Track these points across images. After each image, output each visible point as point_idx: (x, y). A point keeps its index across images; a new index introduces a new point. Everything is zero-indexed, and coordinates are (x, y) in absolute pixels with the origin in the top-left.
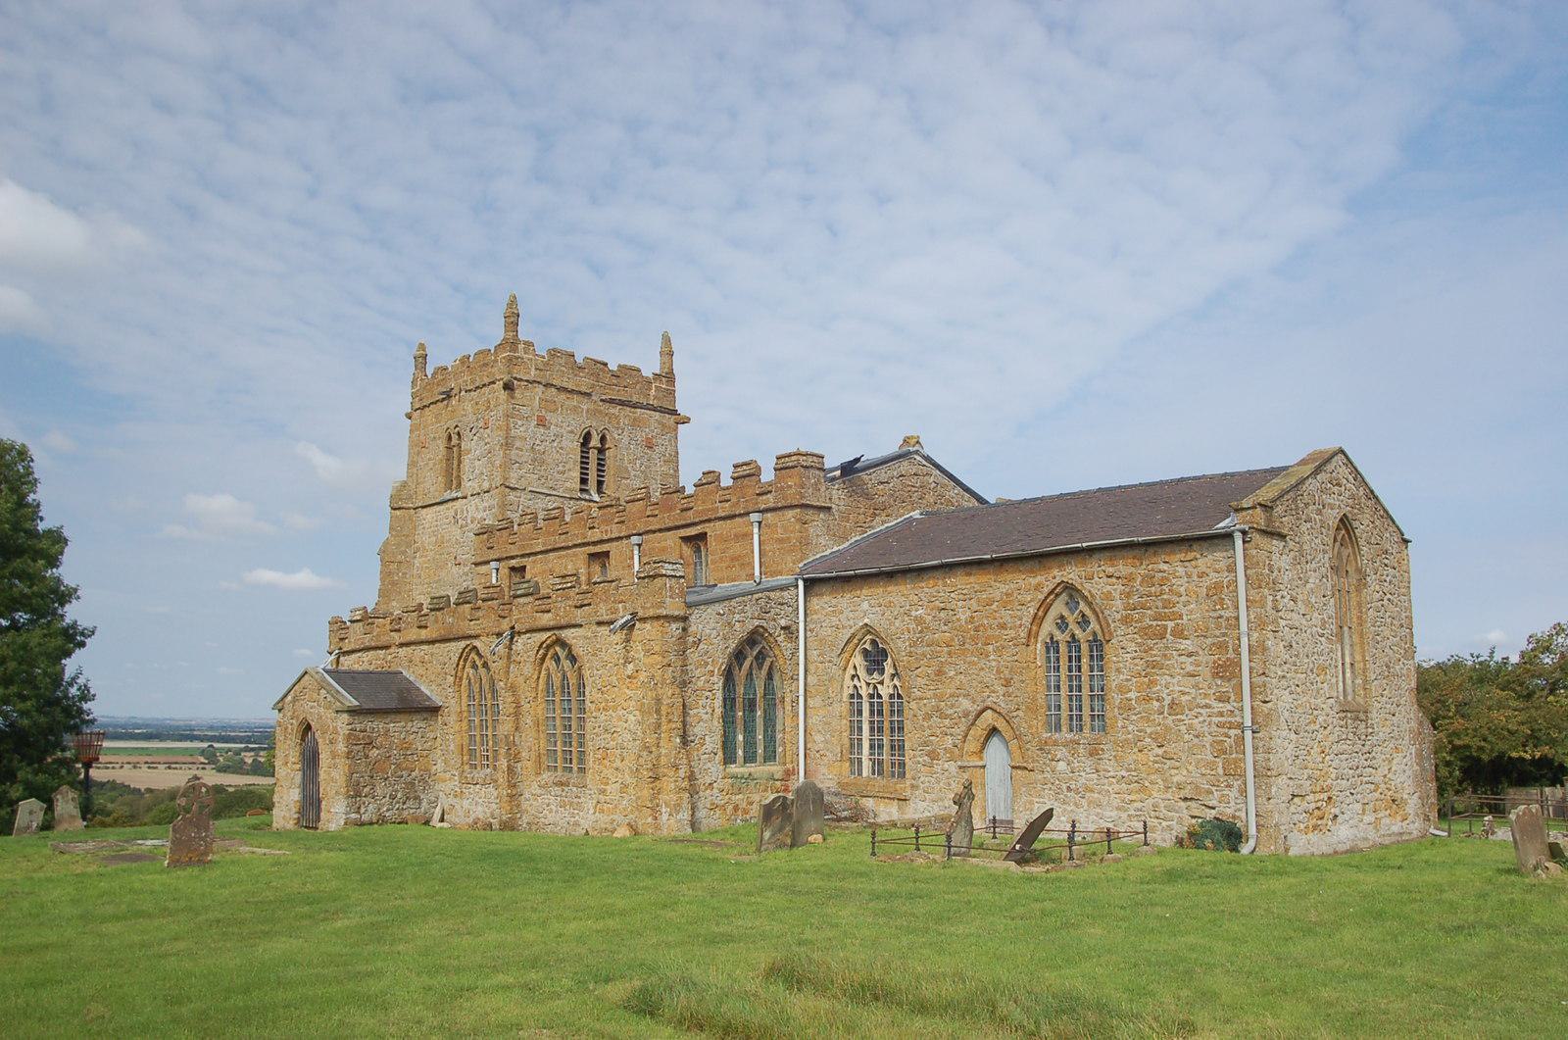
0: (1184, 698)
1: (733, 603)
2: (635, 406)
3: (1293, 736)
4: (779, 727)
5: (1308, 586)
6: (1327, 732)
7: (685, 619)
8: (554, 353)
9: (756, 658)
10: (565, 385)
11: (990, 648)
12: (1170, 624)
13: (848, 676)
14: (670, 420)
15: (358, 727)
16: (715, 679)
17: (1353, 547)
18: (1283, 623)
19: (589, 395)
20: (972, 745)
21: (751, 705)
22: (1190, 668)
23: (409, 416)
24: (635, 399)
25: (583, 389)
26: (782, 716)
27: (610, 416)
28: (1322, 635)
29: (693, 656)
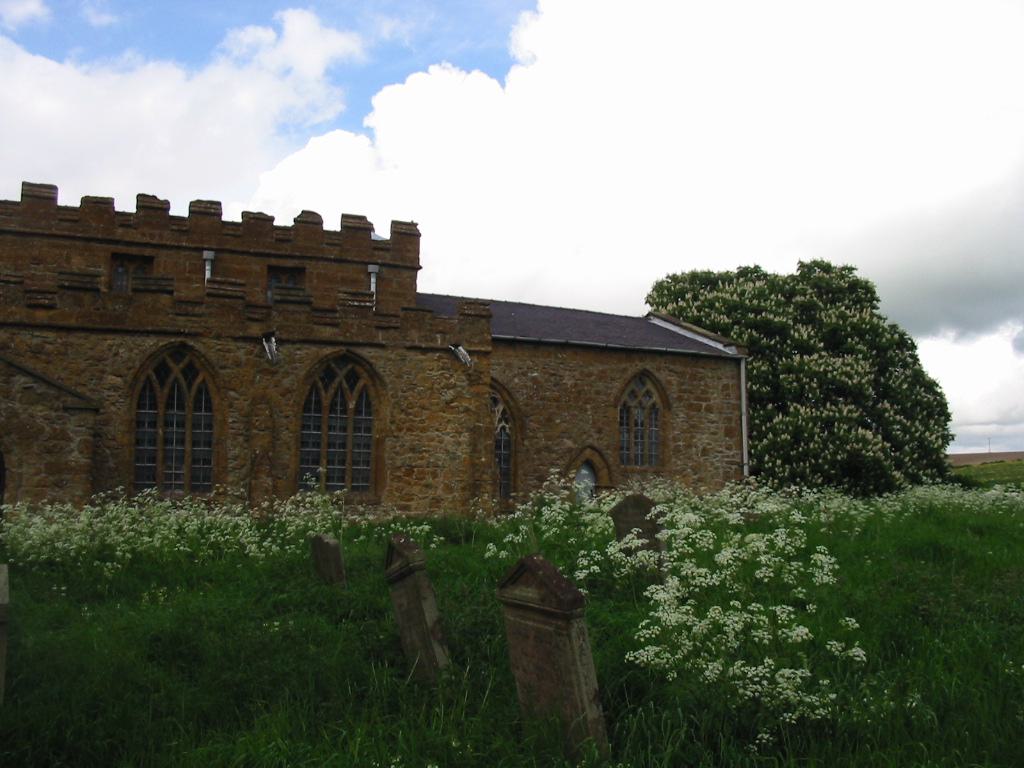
0: (709, 447)
11: (588, 406)
12: (704, 404)
22: (712, 430)
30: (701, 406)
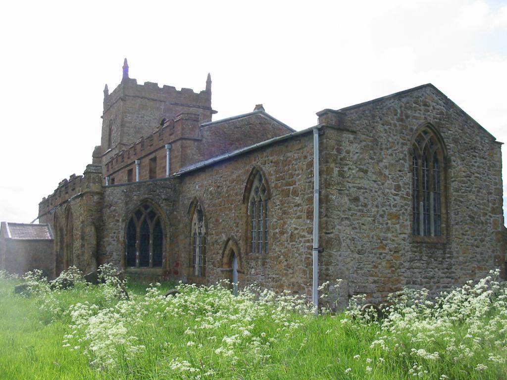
0: (296, 232)
4: (164, 249)
8: (147, 84)
9: (149, 214)
10: (153, 97)
12: (291, 188)
13: (193, 224)
14: (208, 113)
16: (120, 224)
17: (440, 143)
20: (225, 260)
21: (145, 238)
23: (102, 117)
28: (396, 195)
30: (290, 189)
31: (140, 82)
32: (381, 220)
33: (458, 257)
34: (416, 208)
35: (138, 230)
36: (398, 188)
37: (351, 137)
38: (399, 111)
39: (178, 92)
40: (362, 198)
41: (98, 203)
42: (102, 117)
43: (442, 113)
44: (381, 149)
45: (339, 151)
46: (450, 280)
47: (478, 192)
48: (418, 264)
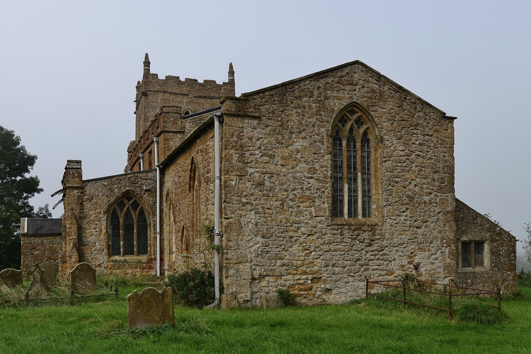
1: (114, 179)
2: (212, 98)
3: (259, 239)
4: (149, 238)
5: (290, 148)
6: (311, 238)
7: (82, 188)
8: (168, 78)
9: (131, 205)
10: (174, 91)
15: (27, 242)
16: (102, 215)
17: (371, 122)
18: (252, 170)
19: (187, 95)
21: (129, 228)
23: (135, 113)
24: (212, 95)
25: (184, 92)
26: (150, 234)
27: (199, 104)
28: (311, 178)
29: (87, 205)
31: (162, 77)
32: (291, 203)
33: (392, 239)
34: (336, 192)
35: (121, 221)
36: (313, 171)
37: (255, 122)
38: (316, 93)
39: (201, 84)
40: (267, 183)
41: (79, 197)
42: (135, 113)
43: (373, 91)
44: (292, 133)
45: (240, 137)
46: (382, 262)
47: (420, 171)
48: (338, 247)
